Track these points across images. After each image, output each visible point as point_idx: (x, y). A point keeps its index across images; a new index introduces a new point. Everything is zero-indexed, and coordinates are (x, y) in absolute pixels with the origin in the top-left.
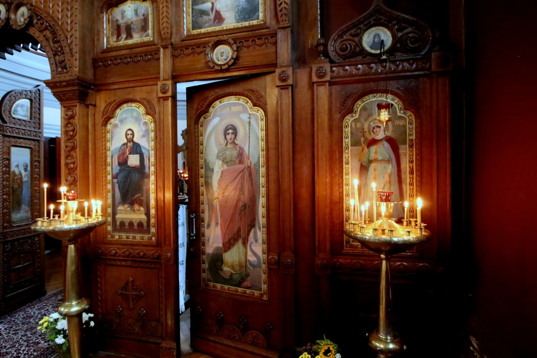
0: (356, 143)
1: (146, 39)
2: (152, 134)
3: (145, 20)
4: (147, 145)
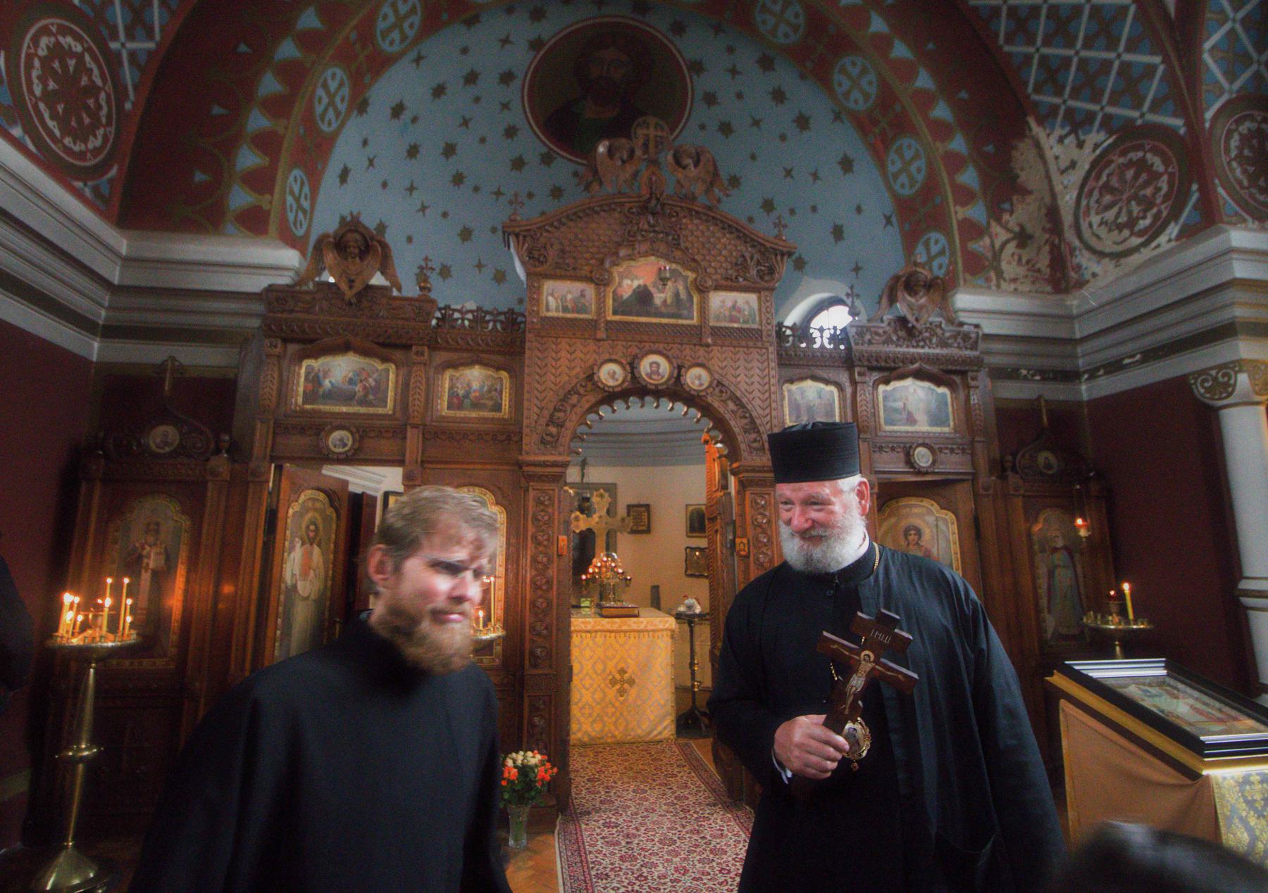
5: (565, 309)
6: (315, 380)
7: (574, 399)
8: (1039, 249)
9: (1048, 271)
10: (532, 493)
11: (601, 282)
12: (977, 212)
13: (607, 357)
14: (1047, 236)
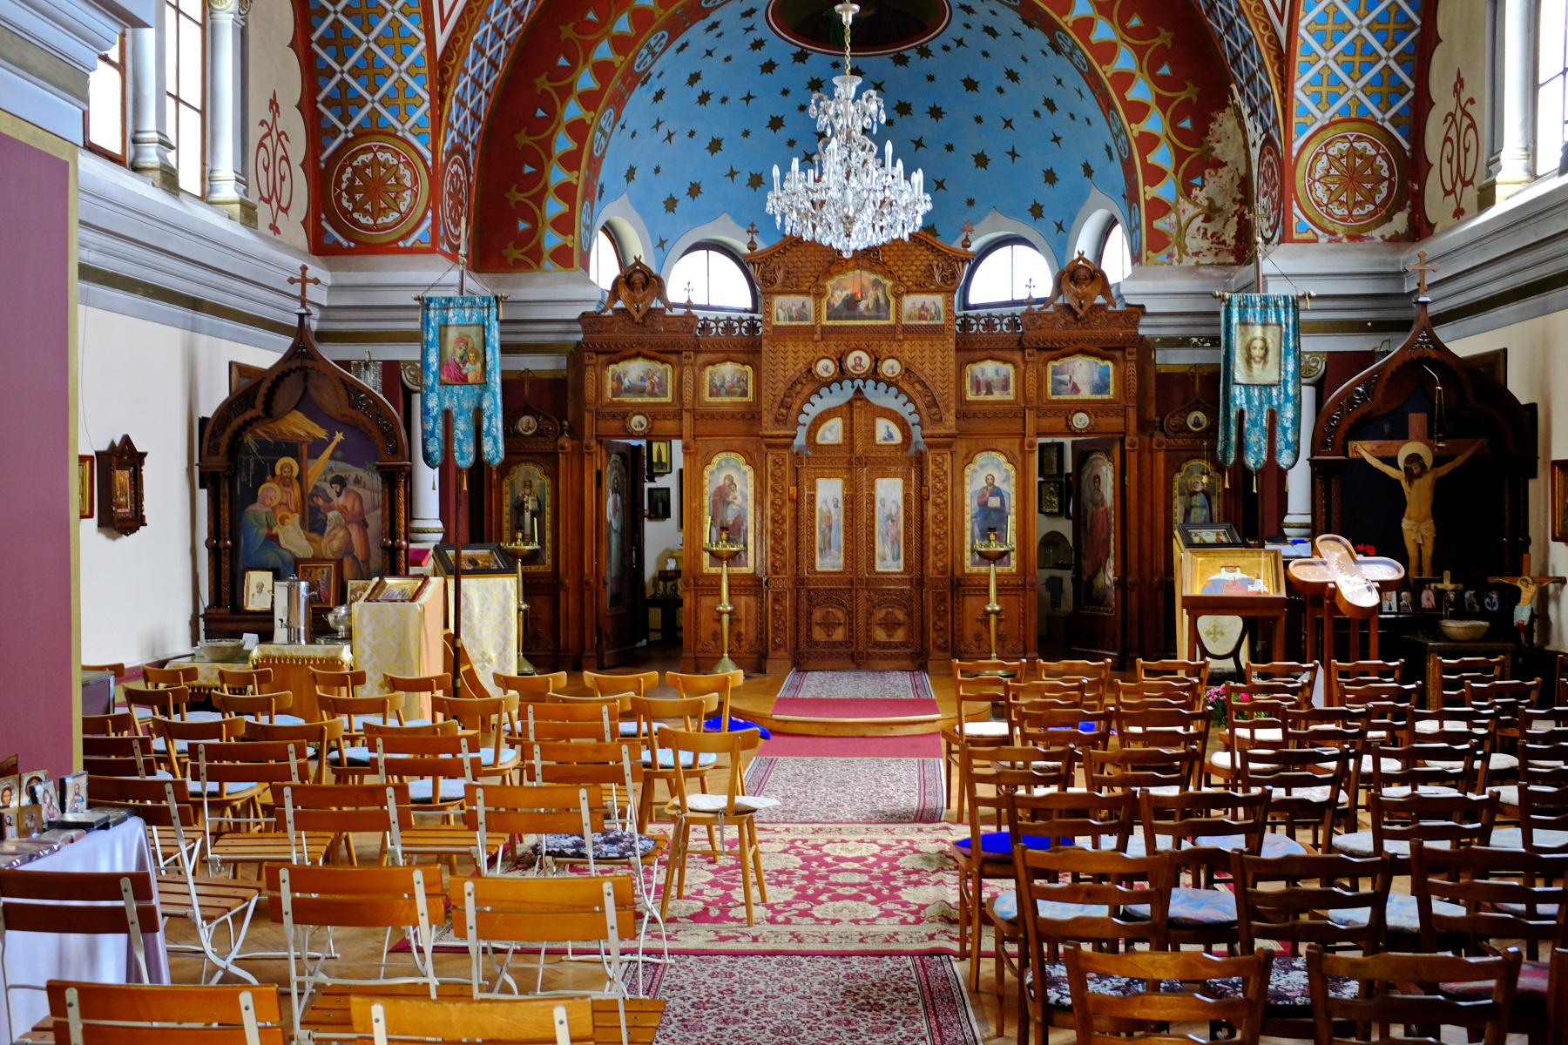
1: (1006, 398)
2: (1013, 481)
3: (1007, 380)
4: (1009, 489)
5: (791, 319)
6: (619, 380)
8: (1227, 220)
9: (1233, 242)
10: (770, 457)
11: (819, 295)
12: (1166, 190)
14: (1236, 207)
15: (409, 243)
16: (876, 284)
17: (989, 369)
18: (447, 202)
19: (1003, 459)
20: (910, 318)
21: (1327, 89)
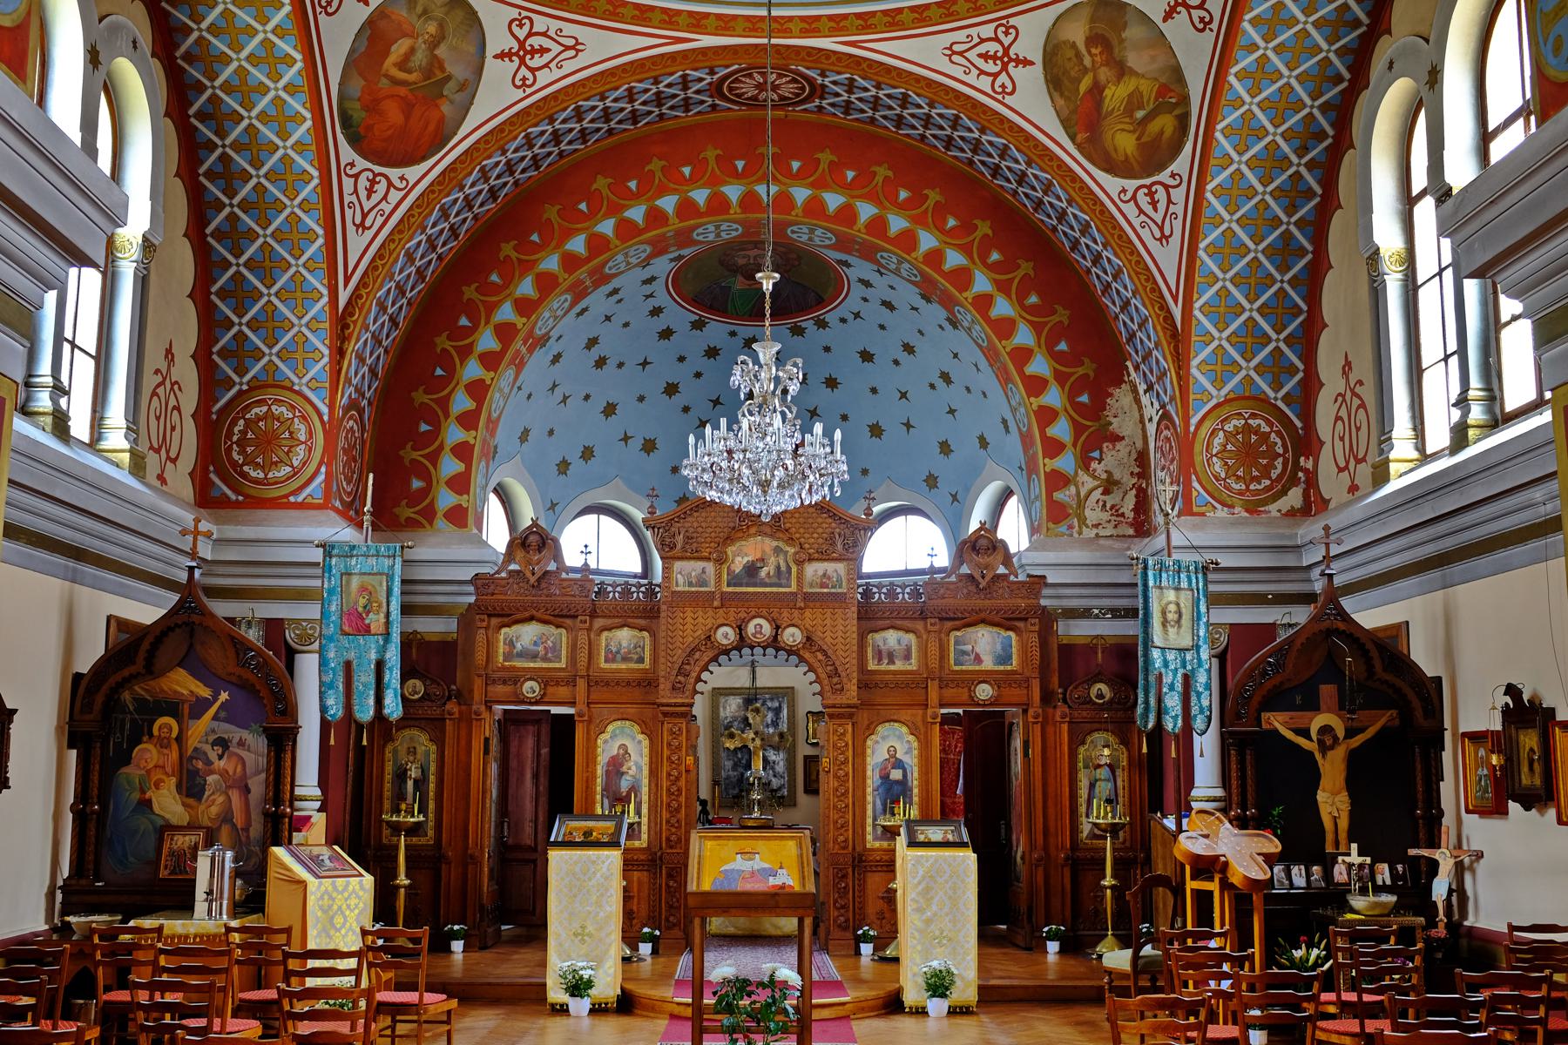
0: (1086, 767)
4: (911, 761)
5: (690, 584)
6: (511, 644)
7: (697, 655)
8: (1125, 493)
13: (720, 621)
14: (1134, 480)
15: (300, 499)
16: (777, 550)
17: (891, 639)
18: (342, 458)
19: (904, 729)
20: (811, 586)
21: (1221, 369)
